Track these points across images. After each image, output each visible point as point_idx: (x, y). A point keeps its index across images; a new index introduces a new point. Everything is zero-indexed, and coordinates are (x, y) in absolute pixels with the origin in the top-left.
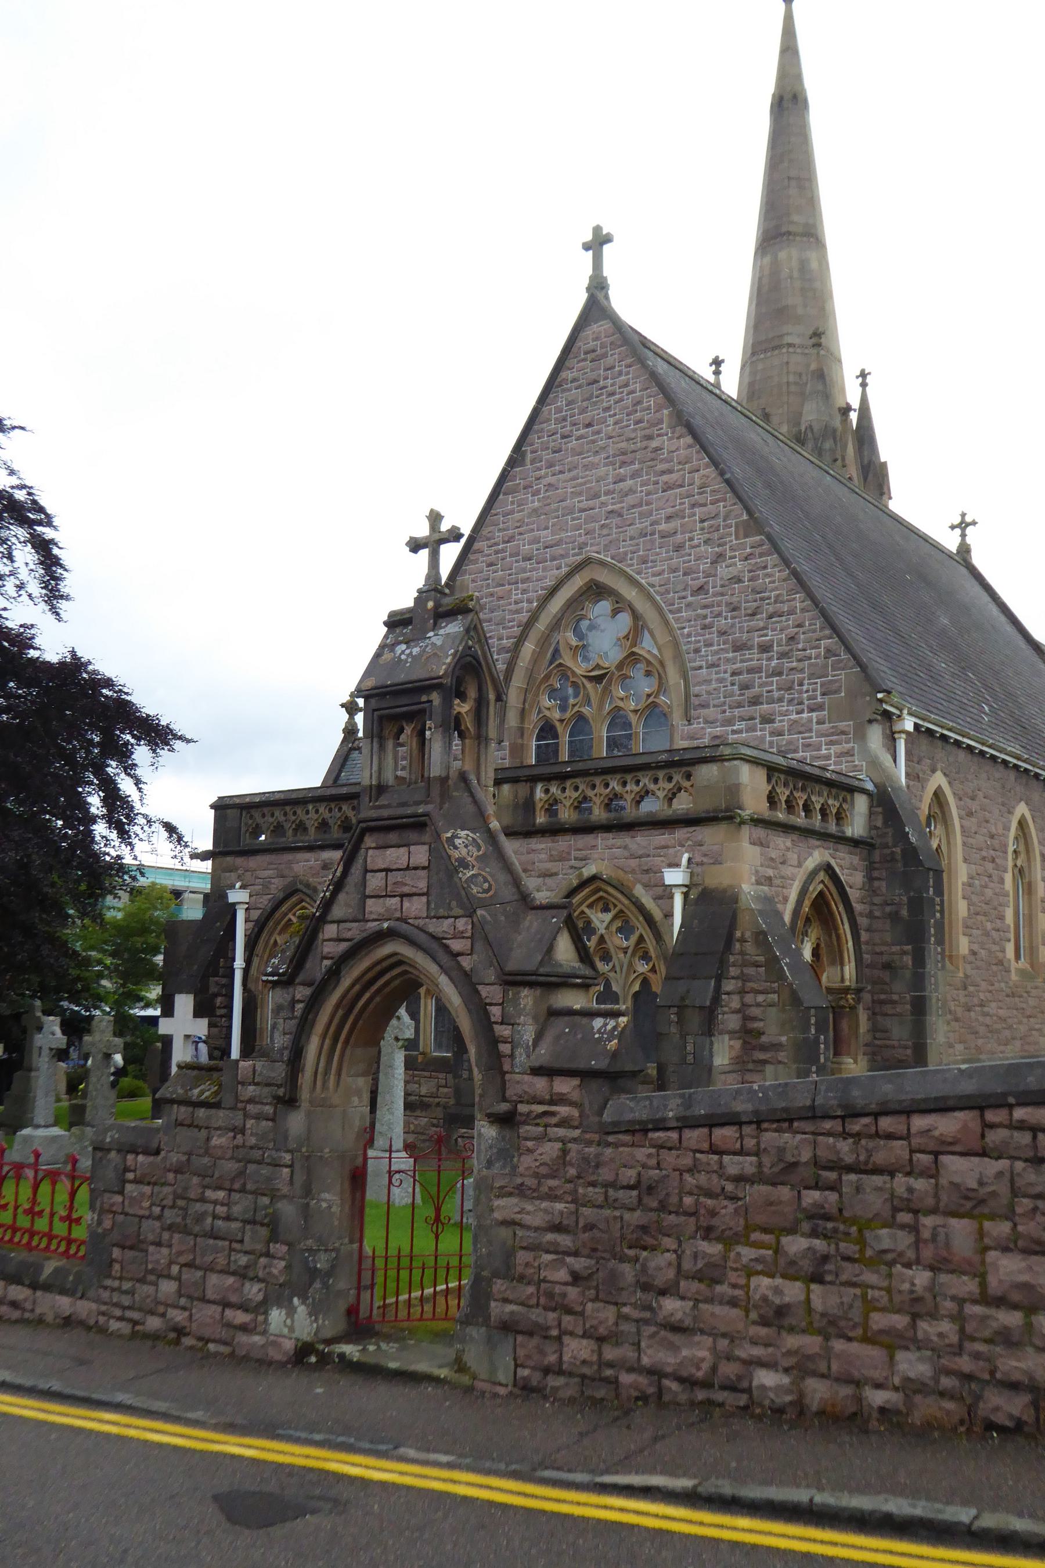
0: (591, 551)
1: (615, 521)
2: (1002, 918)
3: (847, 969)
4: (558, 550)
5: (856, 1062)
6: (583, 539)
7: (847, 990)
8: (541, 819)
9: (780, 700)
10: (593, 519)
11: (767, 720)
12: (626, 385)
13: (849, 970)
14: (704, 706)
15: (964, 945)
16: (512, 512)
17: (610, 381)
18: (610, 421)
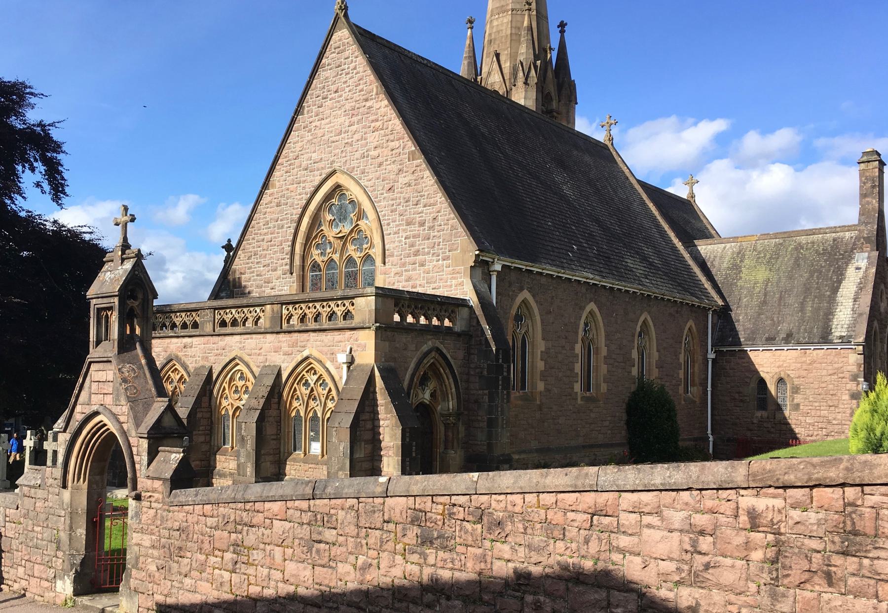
0: (336, 166)
1: (349, 149)
2: (572, 370)
3: (451, 403)
4: (321, 165)
5: (456, 452)
6: (331, 159)
7: (450, 415)
8: (285, 325)
9: (428, 253)
10: (336, 148)
11: (422, 265)
12: (355, 68)
13: (452, 404)
14: (392, 256)
15: (541, 386)
17: (346, 66)
18: (347, 90)
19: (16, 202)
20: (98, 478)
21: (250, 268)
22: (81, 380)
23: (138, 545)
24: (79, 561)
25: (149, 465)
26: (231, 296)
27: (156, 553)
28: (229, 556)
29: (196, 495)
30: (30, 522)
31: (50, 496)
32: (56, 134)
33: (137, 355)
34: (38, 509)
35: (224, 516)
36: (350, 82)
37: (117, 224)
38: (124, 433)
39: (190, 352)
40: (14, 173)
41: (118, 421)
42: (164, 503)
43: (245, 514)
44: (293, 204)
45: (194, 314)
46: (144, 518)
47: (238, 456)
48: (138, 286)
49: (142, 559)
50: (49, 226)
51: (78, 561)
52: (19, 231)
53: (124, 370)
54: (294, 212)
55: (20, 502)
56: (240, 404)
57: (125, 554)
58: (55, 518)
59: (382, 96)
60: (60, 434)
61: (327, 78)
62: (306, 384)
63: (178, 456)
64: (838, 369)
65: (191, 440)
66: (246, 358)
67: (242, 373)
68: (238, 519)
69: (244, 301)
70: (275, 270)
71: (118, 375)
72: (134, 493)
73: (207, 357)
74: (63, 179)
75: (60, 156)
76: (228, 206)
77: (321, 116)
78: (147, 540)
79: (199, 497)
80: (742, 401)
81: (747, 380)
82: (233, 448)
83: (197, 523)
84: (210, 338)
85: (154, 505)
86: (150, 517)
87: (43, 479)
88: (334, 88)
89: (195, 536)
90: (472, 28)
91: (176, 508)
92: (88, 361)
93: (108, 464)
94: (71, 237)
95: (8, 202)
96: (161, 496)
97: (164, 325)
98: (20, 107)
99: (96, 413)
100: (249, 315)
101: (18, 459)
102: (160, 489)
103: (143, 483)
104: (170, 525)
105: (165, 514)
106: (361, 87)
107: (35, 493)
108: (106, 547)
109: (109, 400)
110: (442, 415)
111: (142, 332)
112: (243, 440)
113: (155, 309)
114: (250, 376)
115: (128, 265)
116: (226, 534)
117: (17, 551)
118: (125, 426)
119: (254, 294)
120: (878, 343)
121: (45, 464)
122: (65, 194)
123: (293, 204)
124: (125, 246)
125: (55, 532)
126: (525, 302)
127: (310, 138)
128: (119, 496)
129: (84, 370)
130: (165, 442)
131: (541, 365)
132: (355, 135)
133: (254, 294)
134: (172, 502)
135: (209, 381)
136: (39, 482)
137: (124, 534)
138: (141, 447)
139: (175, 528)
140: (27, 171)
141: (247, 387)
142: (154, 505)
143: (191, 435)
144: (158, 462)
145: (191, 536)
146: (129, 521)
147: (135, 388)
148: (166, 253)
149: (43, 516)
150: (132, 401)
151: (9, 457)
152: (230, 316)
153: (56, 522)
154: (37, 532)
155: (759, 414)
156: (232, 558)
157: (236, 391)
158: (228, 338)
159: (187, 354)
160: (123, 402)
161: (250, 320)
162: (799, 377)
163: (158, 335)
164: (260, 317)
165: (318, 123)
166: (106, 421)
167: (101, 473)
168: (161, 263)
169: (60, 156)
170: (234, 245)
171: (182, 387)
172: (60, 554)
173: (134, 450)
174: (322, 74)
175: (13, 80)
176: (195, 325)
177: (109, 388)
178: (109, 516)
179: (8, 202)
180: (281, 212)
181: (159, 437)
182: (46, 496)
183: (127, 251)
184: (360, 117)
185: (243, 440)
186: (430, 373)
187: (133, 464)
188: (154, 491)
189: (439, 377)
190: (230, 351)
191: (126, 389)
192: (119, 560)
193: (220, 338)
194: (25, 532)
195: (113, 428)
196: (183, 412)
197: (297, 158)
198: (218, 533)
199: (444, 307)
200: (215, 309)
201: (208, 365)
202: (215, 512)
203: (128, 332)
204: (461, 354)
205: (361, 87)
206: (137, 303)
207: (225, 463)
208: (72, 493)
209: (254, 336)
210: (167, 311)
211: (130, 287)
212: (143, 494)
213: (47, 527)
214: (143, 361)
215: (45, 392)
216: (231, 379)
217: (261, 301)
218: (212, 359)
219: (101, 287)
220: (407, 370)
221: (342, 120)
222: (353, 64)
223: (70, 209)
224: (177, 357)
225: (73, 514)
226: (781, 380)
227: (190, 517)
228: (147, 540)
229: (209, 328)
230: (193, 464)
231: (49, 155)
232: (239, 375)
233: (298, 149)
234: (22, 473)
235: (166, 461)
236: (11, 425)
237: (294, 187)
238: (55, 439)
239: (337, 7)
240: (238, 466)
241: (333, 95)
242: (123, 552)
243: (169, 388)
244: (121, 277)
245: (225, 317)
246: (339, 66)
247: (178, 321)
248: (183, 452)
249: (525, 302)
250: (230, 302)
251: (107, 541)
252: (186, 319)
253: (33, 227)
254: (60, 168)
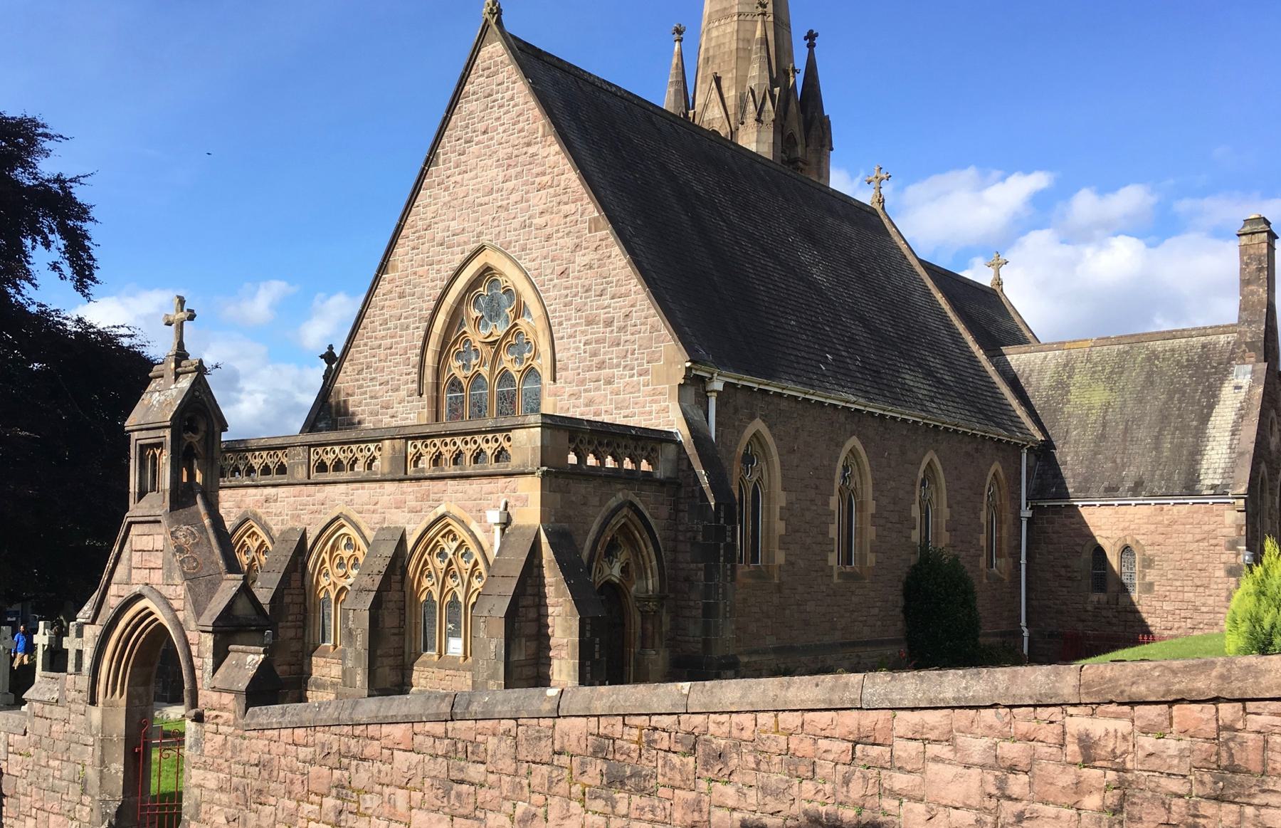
0: (485, 239)
1: (503, 215)
2: (826, 534)
3: (650, 582)
5: (657, 653)
6: (478, 230)
7: (649, 599)
9: (618, 366)
10: (485, 213)
11: (609, 382)
12: (512, 99)
13: (651, 584)
14: (566, 369)
15: (780, 557)
16: (429, 205)
17: (500, 95)
18: (501, 129)
19: (24, 292)
20: (141, 689)
21: (360, 387)
22: (116, 548)
23: (199, 786)
24: (114, 810)
25: (215, 671)
26: (333, 427)
27: (224, 798)
28: (330, 802)
29: (283, 715)
30: (44, 753)
31: (73, 716)
32: (80, 194)
33: (198, 513)
34: (55, 735)
35: (323, 745)
36: (505, 119)
37: (169, 324)
38: (179, 626)
39: (274, 508)
40: (20, 249)
41: (170, 607)
42: (236, 726)
43: (353, 742)
44: (422, 294)
45: (280, 453)
46: (208, 747)
47: (343, 658)
48: (199, 413)
49: (204, 807)
50: (71, 326)
51: (112, 809)
52: (28, 334)
53: (179, 534)
54: (425, 306)
55: (28, 725)
56: (346, 583)
57: (180, 800)
58: (79, 748)
59: (551, 139)
60: (87, 628)
61: (472, 113)
62: (442, 554)
63: (257, 658)
64: (1208, 532)
65: (275, 635)
66: (355, 517)
67: (349, 539)
68: (343, 749)
69: (352, 435)
70: (397, 390)
71: (170, 541)
72: (193, 712)
73: (299, 516)
74: (91, 258)
75: (87, 226)
76: (329, 296)
77: (463, 168)
78: (211, 780)
79: (288, 718)
80: (1069, 578)
81: (1078, 549)
82: (335, 647)
83: (284, 755)
84: (303, 487)
85: (221, 729)
86: (217, 746)
87: (62, 691)
88: (481, 127)
89: (282, 774)
90: (680, 40)
91: (254, 734)
92: (127, 521)
93: (156, 669)
94: (102, 342)
95: (12, 291)
96: (232, 717)
97: (237, 469)
98: (29, 154)
99: (139, 597)
100: (359, 455)
101: (26, 662)
102: (231, 706)
103: (206, 697)
104: (246, 759)
105: (238, 741)
106: (521, 125)
107: (51, 712)
108: (154, 789)
109: (157, 577)
110: (637, 599)
111: (205, 479)
112: (350, 635)
113: (223, 446)
114: (360, 542)
115: (185, 383)
116: (325, 770)
117: (25, 795)
118: (180, 615)
119: (366, 425)
120: (1267, 495)
121: (65, 670)
122: (93, 279)
123: (422, 294)
124: (181, 355)
125: (80, 767)
127: (448, 199)
128: (172, 716)
129: (121, 534)
130: (238, 638)
131: (780, 527)
132: (513, 194)
133: (366, 425)
134: (248, 725)
135: (301, 551)
136: (56, 696)
137: (179, 771)
138: (203, 645)
139: (253, 762)
140: (40, 247)
141: (356, 559)
142: (222, 729)
143: (275, 628)
144: (228, 666)
145: (275, 773)
146: (186, 752)
147: (195, 560)
148: (239, 365)
149: (61, 745)
150: (191, 579)
151: (12, 659)
152: (332, 456)
153: (81, 753)
154: (54, 768)
155: (1095, 597)
156: (335, 806)
157: (341, 565)
158: (328, 488)
159: (270, 511)
160: (178, 580)
161: (361, 462)
162: (1152, 544)
163: (228, 484)
164: (374, 458)
165: (458, 178)
166: (153, 607)
167: (146, 683)
168: (233, 379)
169: (87, 226)
170: (338, 352)
171: (263, 558)
172: (87, 800)
173: (194, 649)
174: (465, 107)
175: (19, 116)
176: (282, 470)
177: (157, 560)
178: (157, 745)
179: (12, 291)
180: (405, 306)
181: (229, 630)
182: (66, 716)
183: (184, 363)
184: (519, 169)
185: (350, 635)
186: (620, 539)
187: (192, 669)
188: (223, 708)
189: (633, 544)
190: (332, 507)
191: (182, 562)
192: (172, 808)
193: (317, 488)
194: (37, 768)
195: (162, 617)
196: (264, 595)
197: (428, 228)
198: (314, 770)
199: (641, 444)
200: (310, 446)
201: (300, 526)
202: (311, 739)
203: (185, 480)
204: (665, 511)
205: (521, 125)
206: (197, 437)
207: (324, 668)
208: (103, 712)
209: (367, 485)
210: (240, 449)
211: (188, 415)
212: (206, 713)
213: (68, 760)
214: (207, 522)
215: (65, 567)
216: (333, 547)
217: (377, 435)
218: (306, 518)
219: (145, 415)
220: (587, 533)
221: (496, 173)
222: (510, 92)
223: (101, 301)
224: (255, 515)
225: (105, 742)
226: (1126, 549)
227: (273, 746)
228: (211, 780)
229: (301, 474)
230: (279, 670)
231: (71, 223)
232: (345, 541)
233: (430, 215)
234: (32, 683)
235: (241, 666)
236: (16, 614)
237: (423, 270)
238: (80, 634)
239: (486, 10)
240: (344, 672)
241: (481, 137)
242: (177, 797)
243: (244, 559)
244: (175, 400)
245: (324, 457)
246: (490, 95)
247: (256, 463)
248: (264, 652)
249: (756, 435)
250: (332, 436)
251: (154, 781)
252: (269, 461)
253: (48, 328)
254: (87, 243)
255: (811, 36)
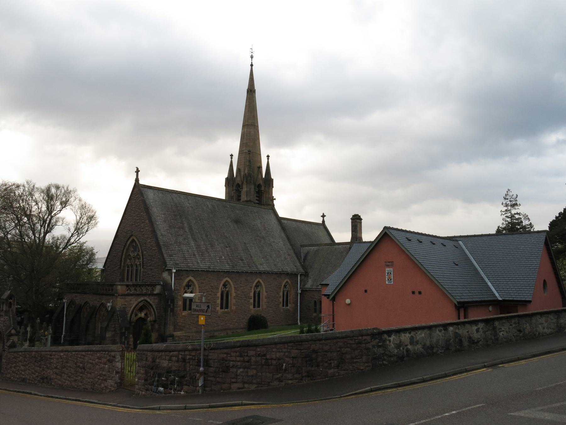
126: (190, 280)
220: (131, 307)
255: (268, 156)
